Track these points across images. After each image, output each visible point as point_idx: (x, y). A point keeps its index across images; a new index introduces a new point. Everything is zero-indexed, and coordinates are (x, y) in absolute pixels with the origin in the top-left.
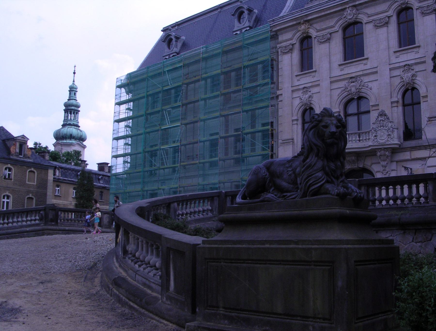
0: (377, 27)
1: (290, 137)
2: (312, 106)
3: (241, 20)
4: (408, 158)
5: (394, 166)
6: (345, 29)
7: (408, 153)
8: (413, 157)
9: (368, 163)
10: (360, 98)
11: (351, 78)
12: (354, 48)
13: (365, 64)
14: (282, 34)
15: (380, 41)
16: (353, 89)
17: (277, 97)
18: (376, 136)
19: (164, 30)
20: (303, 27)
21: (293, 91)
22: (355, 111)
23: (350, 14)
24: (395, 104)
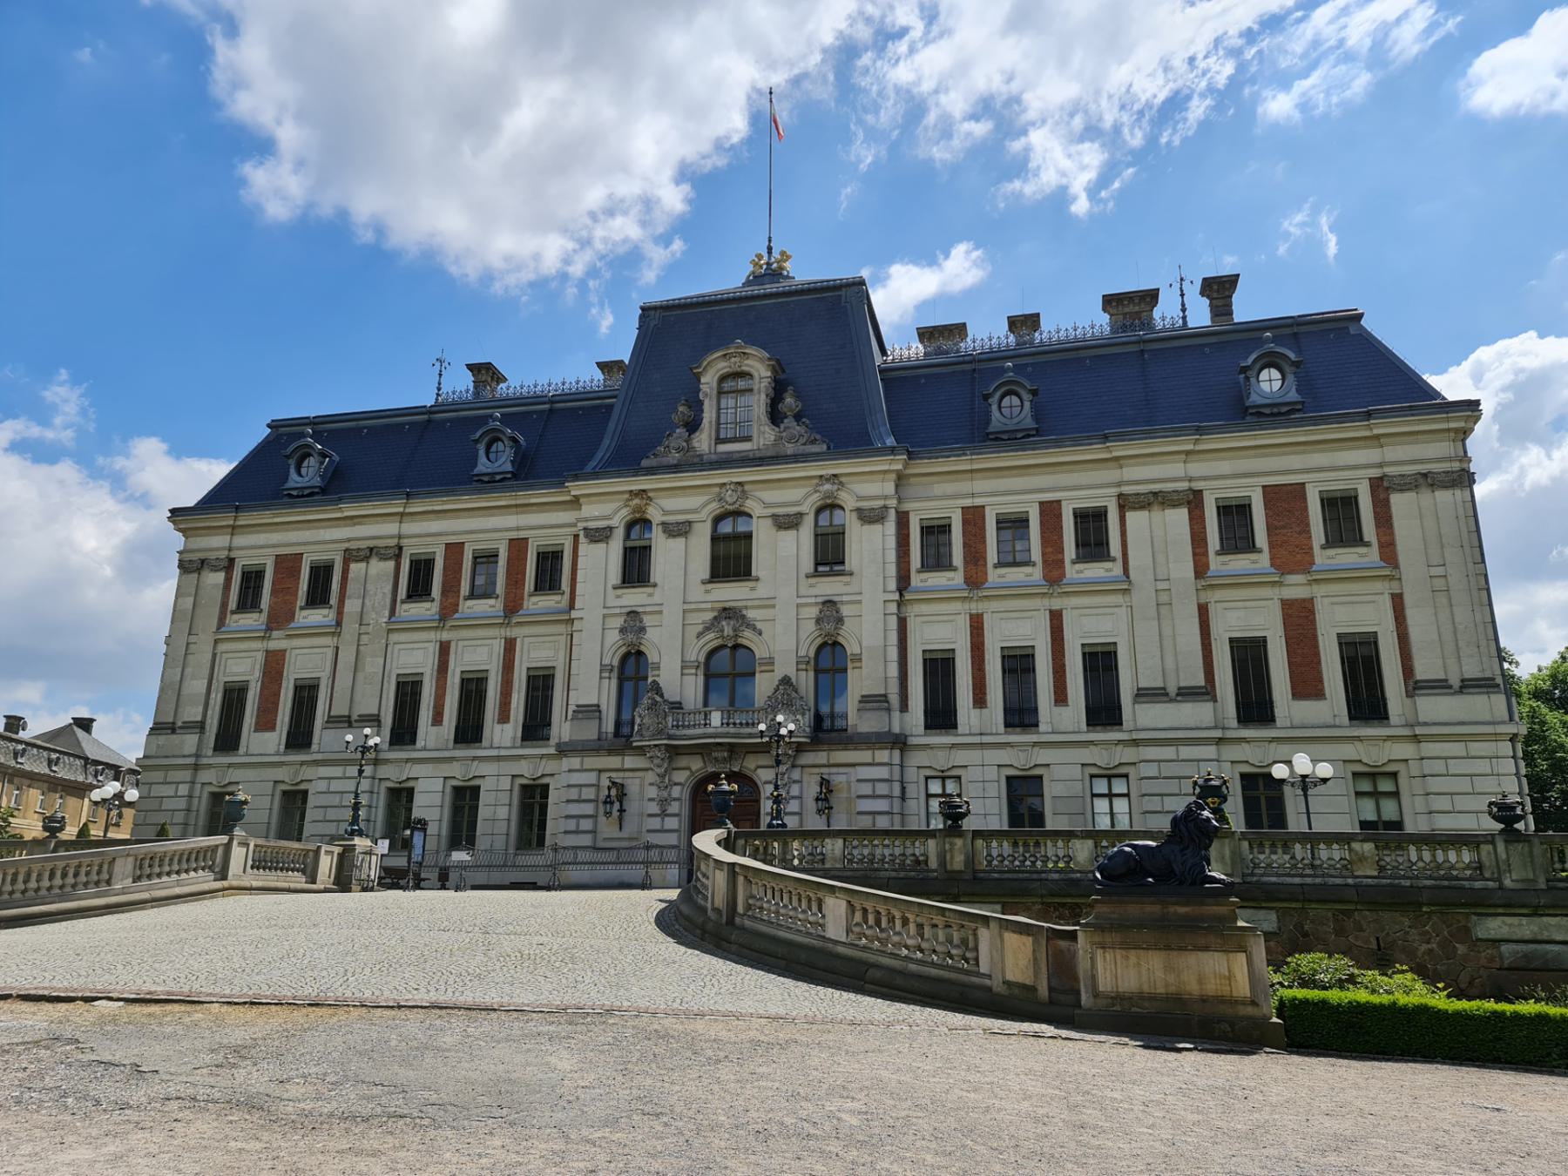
3: (492, 456)
4: (824, 761)
5: (796, 774)
6: (717, 520)
7: (824, 754)
9: (750, 763)
10: (736, 647)
11: (725, 609)
12: (731, 561)
14: (591, 503)
15: (781, 556)
16: (728, 630)
17: (572, 621)
20: (636, 501)
22: (727, 668)
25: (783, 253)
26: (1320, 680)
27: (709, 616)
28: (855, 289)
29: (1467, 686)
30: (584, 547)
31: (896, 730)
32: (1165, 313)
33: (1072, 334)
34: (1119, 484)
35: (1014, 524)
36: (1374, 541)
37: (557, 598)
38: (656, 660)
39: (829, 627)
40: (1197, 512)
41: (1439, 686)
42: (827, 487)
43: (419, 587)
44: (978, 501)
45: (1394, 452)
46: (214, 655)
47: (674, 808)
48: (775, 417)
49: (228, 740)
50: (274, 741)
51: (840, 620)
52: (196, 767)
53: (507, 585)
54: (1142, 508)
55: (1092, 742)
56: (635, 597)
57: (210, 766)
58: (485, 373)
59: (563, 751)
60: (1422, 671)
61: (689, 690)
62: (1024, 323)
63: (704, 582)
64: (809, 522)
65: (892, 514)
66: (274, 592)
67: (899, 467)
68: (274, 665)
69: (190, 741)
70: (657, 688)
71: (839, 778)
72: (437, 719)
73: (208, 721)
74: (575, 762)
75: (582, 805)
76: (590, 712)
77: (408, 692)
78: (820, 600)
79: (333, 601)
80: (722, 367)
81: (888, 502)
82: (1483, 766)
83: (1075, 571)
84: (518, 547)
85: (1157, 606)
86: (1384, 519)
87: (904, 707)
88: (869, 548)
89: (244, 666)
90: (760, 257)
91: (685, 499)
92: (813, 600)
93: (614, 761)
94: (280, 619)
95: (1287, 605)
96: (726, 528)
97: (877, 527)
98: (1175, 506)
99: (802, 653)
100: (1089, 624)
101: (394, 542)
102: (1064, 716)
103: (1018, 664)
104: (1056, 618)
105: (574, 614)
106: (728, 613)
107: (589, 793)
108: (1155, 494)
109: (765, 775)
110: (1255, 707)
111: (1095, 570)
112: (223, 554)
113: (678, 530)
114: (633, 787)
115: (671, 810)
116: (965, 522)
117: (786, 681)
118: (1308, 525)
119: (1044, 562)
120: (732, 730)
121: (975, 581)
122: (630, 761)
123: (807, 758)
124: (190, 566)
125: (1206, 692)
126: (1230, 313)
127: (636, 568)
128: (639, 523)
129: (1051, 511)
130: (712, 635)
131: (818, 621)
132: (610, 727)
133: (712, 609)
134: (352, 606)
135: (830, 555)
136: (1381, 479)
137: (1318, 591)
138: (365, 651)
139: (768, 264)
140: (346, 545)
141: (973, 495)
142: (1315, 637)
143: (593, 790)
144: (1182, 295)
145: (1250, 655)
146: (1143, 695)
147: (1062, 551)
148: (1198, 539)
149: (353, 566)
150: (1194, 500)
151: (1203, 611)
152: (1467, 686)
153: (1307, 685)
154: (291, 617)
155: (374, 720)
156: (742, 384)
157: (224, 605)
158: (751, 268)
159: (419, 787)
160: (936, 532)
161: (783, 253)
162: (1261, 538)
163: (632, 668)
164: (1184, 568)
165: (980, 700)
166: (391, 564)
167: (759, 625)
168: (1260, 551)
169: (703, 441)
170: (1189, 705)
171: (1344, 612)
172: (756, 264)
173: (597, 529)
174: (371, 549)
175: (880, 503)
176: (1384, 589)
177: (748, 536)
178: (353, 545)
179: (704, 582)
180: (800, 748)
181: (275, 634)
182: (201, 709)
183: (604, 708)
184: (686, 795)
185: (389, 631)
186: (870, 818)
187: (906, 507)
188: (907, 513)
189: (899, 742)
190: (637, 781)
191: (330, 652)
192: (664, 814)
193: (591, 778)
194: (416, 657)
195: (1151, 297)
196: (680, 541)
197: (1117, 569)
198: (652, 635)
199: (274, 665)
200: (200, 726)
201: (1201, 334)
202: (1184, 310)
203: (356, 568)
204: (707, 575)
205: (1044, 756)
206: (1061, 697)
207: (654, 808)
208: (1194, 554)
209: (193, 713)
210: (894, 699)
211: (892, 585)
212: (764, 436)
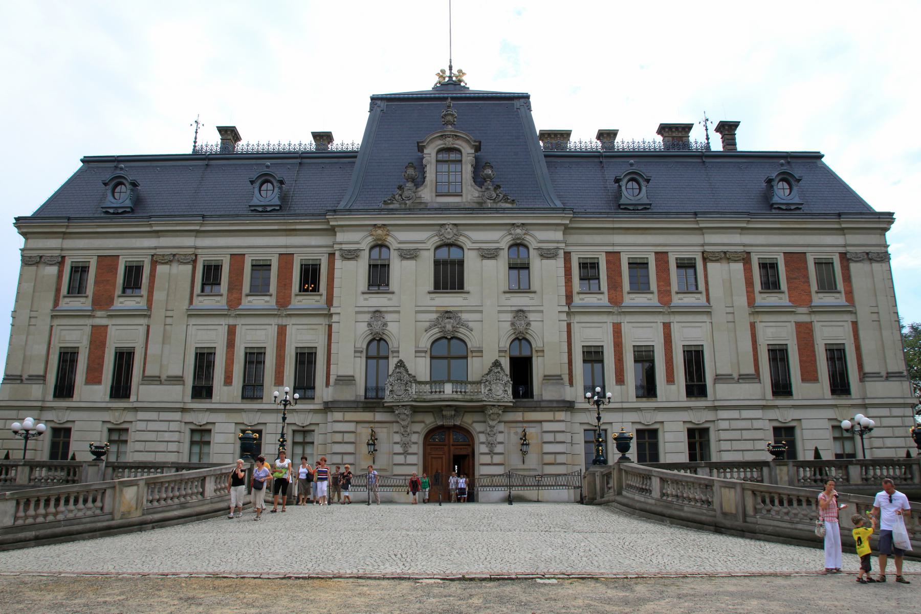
0: (484, 257)
1: (351, 373)
2: (385, 337)
4: (521, 419)
5: (501, 427)
7: (520, 414)
8: (526, 419)
9: (468, 420)
11: (447, 312)
12: (449, 276)
13: (465, 299)
15: (485, 276)
17: (331, 315)
18: (490, 390)
19: (86, 160)
21: (357, 313)
23: (449, 233)
24: (503, 354)
25: (460, 71)
26: (816, 371)
27: (434, 316)
28: (522, 101)
29: (889, 376)
30: (338, 263)
31: (568, 399)
32: (696, 137)
33: (642, 145)
34: (703, 245)
35: (638, 265)
36: (843, 290)
37: (318, 298)
38: (396, 345)
39: (522, 329)
40: (747, 266)
41: (876, 376)
42: (518, 231)
44: (617, 249)
45: (852, 239)
46: (52, 327)
47: (414, 449)
48: (479, 179)
49: (64, 389)
50: (101, 392)
51: (528, 324)
52: (42, 409)
53: (278, 286)
54: (717, 261)
55: (689, 408)
56: (378, 301)
57: (52, 408)
58: (229, 134)
59: (328, 407)
60: (867, 369)
61: (421, 368)
62: (607, 136)
63: (429, 293)
64: (504, 254)
65: (561, 253)
66: (96, 283)
67: (568, 222)
68: (98, 337)
69: (36, 391)
70: (401, 364)
71: (532, 431)
72: (228, 381)
73: (48, 376)
74: (338, 416)
75: (346, 446)
76: (347, 380)
77: (204, 361)
78: (514, 309)
79: (144, 291)
80: (439, 144)
81: (559, 245)
82: (897, 422)
83: (677, 300)
84: (286, 259)
85: (725, 323)
86: (847, 278)
87: (571, 384)
88: (547, 274)
89: (77, 336)
90: (443, 71)
92: (509, 309)
93: (368, 416)
94: (102, 301)
95: (798, 325)
96: (443, 254)
97: (551, 262)
98: (736, 261)
99: (502, 345)
100: (687, 333)
101: (191, 251)
102: (672, 390)
103: (644, 357)
104: (667, 327)
105: (333, 310)
106: (447, 314)
107: (349, 437)
108: (725, 253)
109: (478, 427)
110: (782, 388)
111: (689, 300)
112: (57, 253)
113: (409, 255)
114: (382, 433)
115: (410, 451)
116: (608, 262)
117: (497, 364)
118: (808, 278)
119: (659, 291)
120: (460, 397)
121: (616, 300)
122: (379, 416)
123: (511, 416)
124: (29, 260)
125: (755, 377)
126: (735, 144)
128: (380, 245)
129: (662, 257)
130: (436, 330)
131: (513, 324)
132: (362, 393)
133: (437, 312)
134: (158, 295)
136: (845, 254)
137: (814, 318)
139: (450, 77)
140: (153, 252)
141: (613, 245)
142: (813, 346)
143: (352, 435)
144: (707, 130)
145: (778, 355)
146: (719, 378)
147: (669, 285)
148: (749, 283)
149: (160, 269)
150: (746, 259)
151: (753, 326)
152: (889, 376)
153: (809, 375)
154: (111, 302)
155: (178, 380)
156: (453, 156)
157: (58, 290)
158: (436, 79)
159: (217, 428)
160: (589, 269)
161: (460, 71)
162: (784, 285)
164: (741, 300)
165: (620, 380)
166: (189, 267)
167: (471, 324)
168: (783, 292)
169: (427, 194)
170: (747, 385)
171: (829, 332)
172: (441, 76)
173: (349, 251)
174: (174, 255)
175: (555, 245)
176: (849, 318)
177: (461, 263)
178: (159, 252)
179: (429, 293)
180: (506, 409)
181: (99, 313)
182: (43, 366)
183: (357, 378)
184: (421, 442)
185: (189, 316)
186: (553, 456)
187: (569, 249)
188: (570, 253)
189: (569, 406)
190: (385, 430)
191: (142, 330)
192: (406, 453)
193: (351, 427)
194: (212, 335)
195: (688, 128)
196: (410, 264)
197: (702, 300)
198: (392, 328)
199: (98, 337)
200: (43, 378)
201: (717, 155)
202: (708, 139)
203: (160, 269)
204: (432, 288)
205: (660, 417)
206: (670, 379)
207: (398, 449)
208: (747, 292)
209: (37, 369)
210: (566, 378)
211: (563, 301)
212: (471, 194)
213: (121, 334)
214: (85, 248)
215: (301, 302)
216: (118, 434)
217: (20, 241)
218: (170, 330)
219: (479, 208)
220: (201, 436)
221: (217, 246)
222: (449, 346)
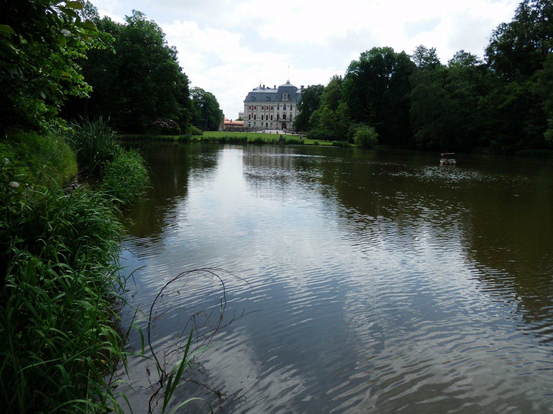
12: (285, 108)
15: (288, 108)
43: (263, 109)
49: (250, 119)
50: (253, 119)
61: (282, 118)
68: (252, 113)
77: (262, 116)
88: (294, 108)
89: (250, 113)
91: (282, 104)
94: (252, 110)
127: (278, 109)
128: (278, 105)
135: (291, 109)
138: (259, 113)
163: (278, 116)
194: (263, 114)
199: (252, 113)
212: (287, 100)
213: (254, 113)
214: (250, 104)
215: (271, 111)
216: (255, 123)
217: (243, 103)
218: (259, 113)
219: (288, 101)
220: (262, 123)
221: (263, 104)
222: (284, 117)
